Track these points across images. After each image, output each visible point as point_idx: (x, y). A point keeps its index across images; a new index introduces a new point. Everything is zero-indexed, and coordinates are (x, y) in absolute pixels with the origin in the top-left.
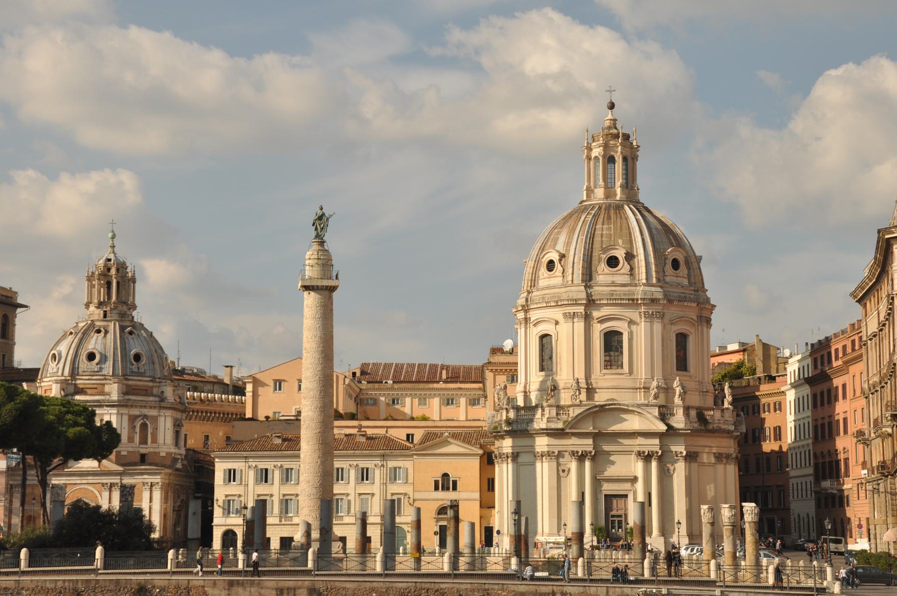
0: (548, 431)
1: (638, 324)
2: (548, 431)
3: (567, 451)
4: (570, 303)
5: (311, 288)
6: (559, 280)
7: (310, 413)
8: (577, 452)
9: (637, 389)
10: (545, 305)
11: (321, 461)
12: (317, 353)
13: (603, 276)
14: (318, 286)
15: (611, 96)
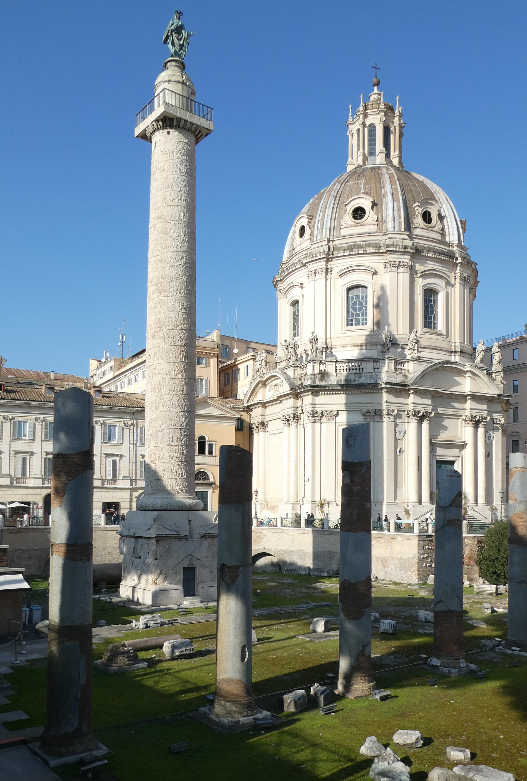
0: (392, 386)
1: (453, 286)
2: (392, 386)
3: (404, 411)
4: (398, 250)
5: (175, 124)
6: (373, 228)
7: (172, 315)
8: (419, 412)
9: (451, 352)
10: (361, 251)
11: (187, 390)
12: (182, 225)
13: (421, 230)
14: (186, 121)
15: (376, 74)
